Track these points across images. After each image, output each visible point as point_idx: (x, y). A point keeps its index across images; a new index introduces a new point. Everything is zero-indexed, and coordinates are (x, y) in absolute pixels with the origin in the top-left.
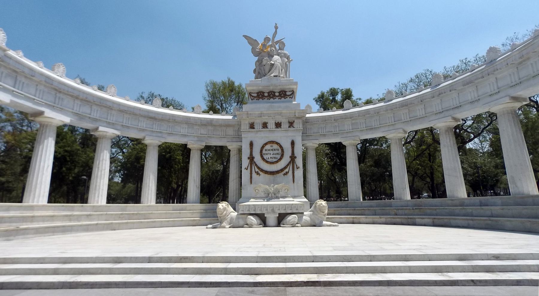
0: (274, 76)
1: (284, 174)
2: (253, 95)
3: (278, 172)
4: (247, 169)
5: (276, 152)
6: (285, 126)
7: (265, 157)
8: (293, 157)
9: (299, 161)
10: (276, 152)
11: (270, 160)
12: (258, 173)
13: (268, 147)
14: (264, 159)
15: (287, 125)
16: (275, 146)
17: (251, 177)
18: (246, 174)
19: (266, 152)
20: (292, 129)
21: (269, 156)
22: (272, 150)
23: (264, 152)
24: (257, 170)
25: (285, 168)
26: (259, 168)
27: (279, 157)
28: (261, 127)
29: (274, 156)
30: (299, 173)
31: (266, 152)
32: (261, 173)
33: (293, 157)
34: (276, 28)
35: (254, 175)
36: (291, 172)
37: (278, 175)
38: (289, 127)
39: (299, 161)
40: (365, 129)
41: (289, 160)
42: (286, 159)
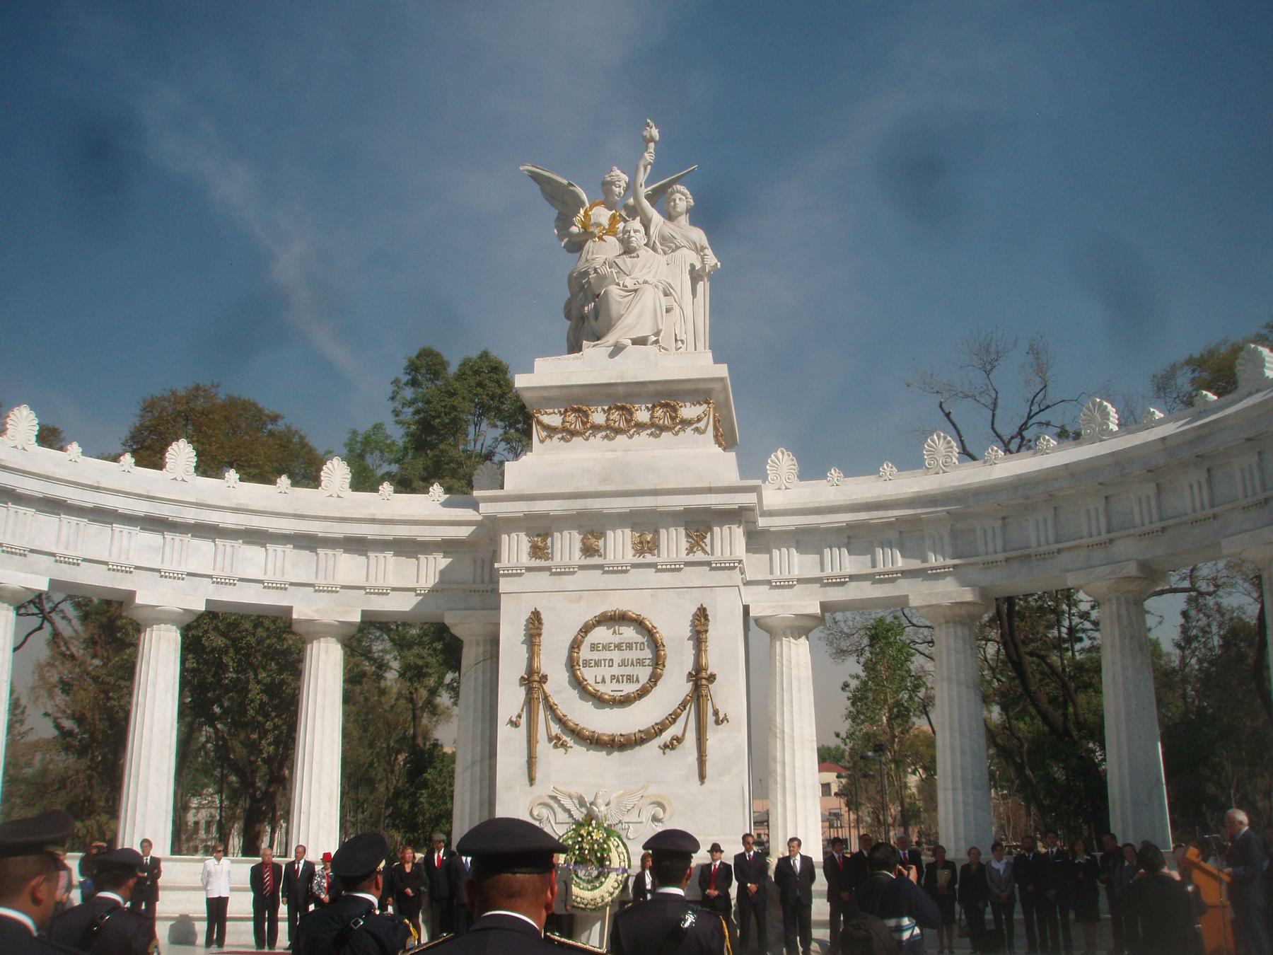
0: (636, 342)
1: (666, 747)
2: (546, 419)
4: (515, 724)
5: (633, 655)
7: (589, 675)
8: (700, 679)
9: (730, 694)
10: (633, 655)
12: (557, 742)
13: (601, 634)
15: (684, 544)
18: (510, 744)
19: (596, 656)
20: (699, 556)
21: (607, 672)
22: (618, 647)
23: (585, 653)
24: (556, 729)
25: (673, 718)
26: (561, 721)
27: (644, 674)
28: (577, 554)
29: (628, 670)
30: (728, 743)
31: (596, 656)
32: (570, 742)
33: (700, 679)
35: (543, 746)
36: (691, 737)
37: (639, 751)
38: (690, 550)
40: (1001, 556)
41: (687, 687)
42: (675, 686)
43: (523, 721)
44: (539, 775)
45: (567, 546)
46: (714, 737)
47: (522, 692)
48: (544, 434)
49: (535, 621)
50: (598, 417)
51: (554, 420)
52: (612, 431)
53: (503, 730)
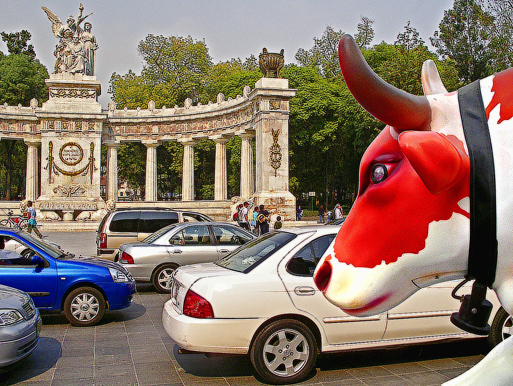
2: (53, 91)
3: (76, 174)
6: (85, 127)
7: (65, 157)
8: (92, 159)
11: (69, 161)
12: (56, 173)
13: (68, 148)
14: (61, 158)
16: (75, 148)
17: (50, 178)
18: (45, 174)
21: (68, 157)
26: (57, 168)
27: (78, 158)
30: (97, 175)
34: (82, 10)
35: (53, 174)
38: (89, 129)
39: (97, 163)
41: (87, 161)
42: (86, 161)
43: (48, 168)
44: (52, 181)
45: (58, 125)
46: (94, 174)
47: (47, 162)
48: (53, 95)
49: (51, 143)
50: (67, 92)
51: (55, 92)
52: (70, 96)
53: (43, 170)
